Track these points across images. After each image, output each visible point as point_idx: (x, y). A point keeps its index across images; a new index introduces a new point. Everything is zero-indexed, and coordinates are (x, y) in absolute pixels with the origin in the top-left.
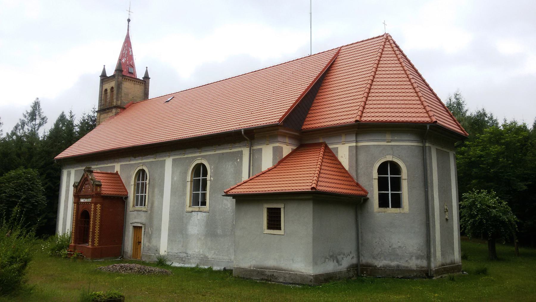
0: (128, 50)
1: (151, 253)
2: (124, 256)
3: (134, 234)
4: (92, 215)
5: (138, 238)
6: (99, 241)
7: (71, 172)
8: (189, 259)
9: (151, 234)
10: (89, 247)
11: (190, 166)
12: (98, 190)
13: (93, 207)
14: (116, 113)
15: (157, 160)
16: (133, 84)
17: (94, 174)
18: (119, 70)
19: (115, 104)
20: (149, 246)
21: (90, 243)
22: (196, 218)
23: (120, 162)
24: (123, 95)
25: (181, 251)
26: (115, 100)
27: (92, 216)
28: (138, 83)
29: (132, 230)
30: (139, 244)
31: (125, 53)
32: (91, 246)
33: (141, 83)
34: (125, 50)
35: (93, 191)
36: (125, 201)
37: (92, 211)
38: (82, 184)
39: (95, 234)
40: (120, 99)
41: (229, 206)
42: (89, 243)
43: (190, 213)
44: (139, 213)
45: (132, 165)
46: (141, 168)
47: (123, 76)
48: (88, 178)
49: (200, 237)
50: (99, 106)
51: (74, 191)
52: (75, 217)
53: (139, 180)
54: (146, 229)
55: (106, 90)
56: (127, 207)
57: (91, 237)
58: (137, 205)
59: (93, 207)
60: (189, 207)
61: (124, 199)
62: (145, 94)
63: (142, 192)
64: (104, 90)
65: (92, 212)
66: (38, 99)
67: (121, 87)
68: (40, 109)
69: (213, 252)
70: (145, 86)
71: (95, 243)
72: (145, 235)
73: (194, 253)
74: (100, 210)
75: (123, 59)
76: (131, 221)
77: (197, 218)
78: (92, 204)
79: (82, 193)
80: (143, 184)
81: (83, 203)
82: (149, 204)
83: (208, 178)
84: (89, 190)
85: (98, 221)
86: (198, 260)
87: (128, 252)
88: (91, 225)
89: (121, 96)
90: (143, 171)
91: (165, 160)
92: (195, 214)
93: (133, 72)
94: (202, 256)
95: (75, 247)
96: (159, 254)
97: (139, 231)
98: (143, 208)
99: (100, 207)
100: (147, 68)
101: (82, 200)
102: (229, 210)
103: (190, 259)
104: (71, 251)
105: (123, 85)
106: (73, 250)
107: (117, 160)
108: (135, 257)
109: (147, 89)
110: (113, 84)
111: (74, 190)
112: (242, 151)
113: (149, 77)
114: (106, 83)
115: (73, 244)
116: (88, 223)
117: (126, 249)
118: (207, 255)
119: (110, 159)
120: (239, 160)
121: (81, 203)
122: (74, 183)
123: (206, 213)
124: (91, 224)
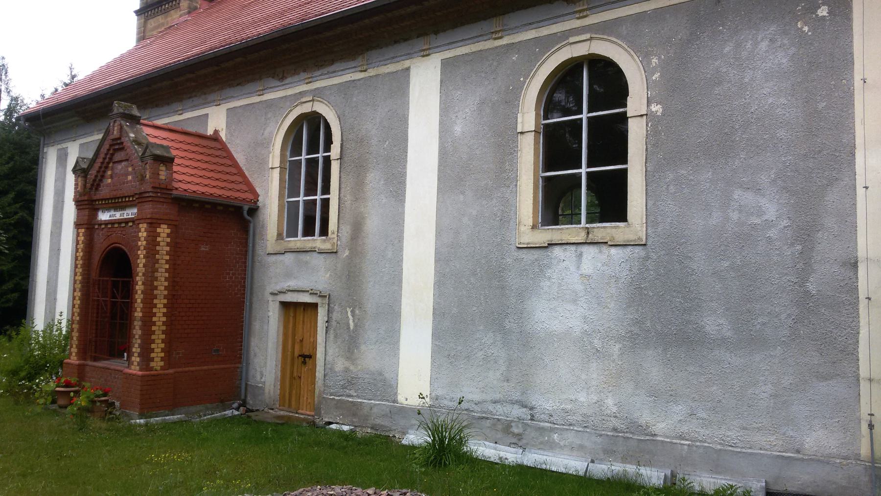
1: (359, 397)
2: (250, 400)
3: (286, 327)
4: (142, 261)
5: (301, 341)
6: (168, 351)
7: (69, 151)
8: (542, 429)
9: (355, 330)
10: (134, 372)
11: (528, 74)
12: (163, 174)
13: (145, 234)
14: (189, 7)
15: (372, 72)
17: (147, 131)
20: (347, 370)
21: (136, 359)
22: (573, 268)
25: (498, 396)
27: (141, 265)
29: (277, 315)
30: (304, 363)
32: (141, 370)
35: (143, 178)
36: (250, 222)
37: (142, 248)
38: (102, 163)
39: (154, 328)
41: (771, 211)
42: (133, 359)
43: (536, 254)
44: (306, 257)
45: (270, 104)
46: (306, 108)
49: (597, 343)
51: (76, 188)
52: (79, 270)
53: (296, 150)
54: (334, 313)
56: (257, 240)
57: (137, 337)
58: (292, 233)
59: (143, 234)
61: (245, 213)
63: (311, 189)
65: (141, 253)
66: (3, 58)
68: (8, 79)
69: (679, 410)
71: (152, 360)
72: (331, 332)
73: (569, 407)
74: (168, 244)
77: (578, 268)
78: (141, 226)
79: (104, 192)
80: (312, 164)
81: (106, 223)
82: (342, 227)
84: (130, 178)
86: (599, 440)
87: (262, 389)
88: (139, 297)
90: (314, 121)
91: (410, 67)
92: (568, 254)
94: (615, 423)
95: (81, 371)
96: (395, 401)
97: (303, 322)
98: (317, 242)
99: (168, 235)
101: (104, 216)
102: (772, 233)
103: (552, 430)
104: (68, 384)
106: (73, 380)
107: (211, 97)
108: (290, 406)
111: (76, 185)
115: (74, 360)
116: (128, 290)
117: (254, 377)
118: (645, 417)
119: (190, 98)
120: (823, 12)
121: (101, 223)
122: (77, 162)
123: (630, 247)
124: (139, 292)
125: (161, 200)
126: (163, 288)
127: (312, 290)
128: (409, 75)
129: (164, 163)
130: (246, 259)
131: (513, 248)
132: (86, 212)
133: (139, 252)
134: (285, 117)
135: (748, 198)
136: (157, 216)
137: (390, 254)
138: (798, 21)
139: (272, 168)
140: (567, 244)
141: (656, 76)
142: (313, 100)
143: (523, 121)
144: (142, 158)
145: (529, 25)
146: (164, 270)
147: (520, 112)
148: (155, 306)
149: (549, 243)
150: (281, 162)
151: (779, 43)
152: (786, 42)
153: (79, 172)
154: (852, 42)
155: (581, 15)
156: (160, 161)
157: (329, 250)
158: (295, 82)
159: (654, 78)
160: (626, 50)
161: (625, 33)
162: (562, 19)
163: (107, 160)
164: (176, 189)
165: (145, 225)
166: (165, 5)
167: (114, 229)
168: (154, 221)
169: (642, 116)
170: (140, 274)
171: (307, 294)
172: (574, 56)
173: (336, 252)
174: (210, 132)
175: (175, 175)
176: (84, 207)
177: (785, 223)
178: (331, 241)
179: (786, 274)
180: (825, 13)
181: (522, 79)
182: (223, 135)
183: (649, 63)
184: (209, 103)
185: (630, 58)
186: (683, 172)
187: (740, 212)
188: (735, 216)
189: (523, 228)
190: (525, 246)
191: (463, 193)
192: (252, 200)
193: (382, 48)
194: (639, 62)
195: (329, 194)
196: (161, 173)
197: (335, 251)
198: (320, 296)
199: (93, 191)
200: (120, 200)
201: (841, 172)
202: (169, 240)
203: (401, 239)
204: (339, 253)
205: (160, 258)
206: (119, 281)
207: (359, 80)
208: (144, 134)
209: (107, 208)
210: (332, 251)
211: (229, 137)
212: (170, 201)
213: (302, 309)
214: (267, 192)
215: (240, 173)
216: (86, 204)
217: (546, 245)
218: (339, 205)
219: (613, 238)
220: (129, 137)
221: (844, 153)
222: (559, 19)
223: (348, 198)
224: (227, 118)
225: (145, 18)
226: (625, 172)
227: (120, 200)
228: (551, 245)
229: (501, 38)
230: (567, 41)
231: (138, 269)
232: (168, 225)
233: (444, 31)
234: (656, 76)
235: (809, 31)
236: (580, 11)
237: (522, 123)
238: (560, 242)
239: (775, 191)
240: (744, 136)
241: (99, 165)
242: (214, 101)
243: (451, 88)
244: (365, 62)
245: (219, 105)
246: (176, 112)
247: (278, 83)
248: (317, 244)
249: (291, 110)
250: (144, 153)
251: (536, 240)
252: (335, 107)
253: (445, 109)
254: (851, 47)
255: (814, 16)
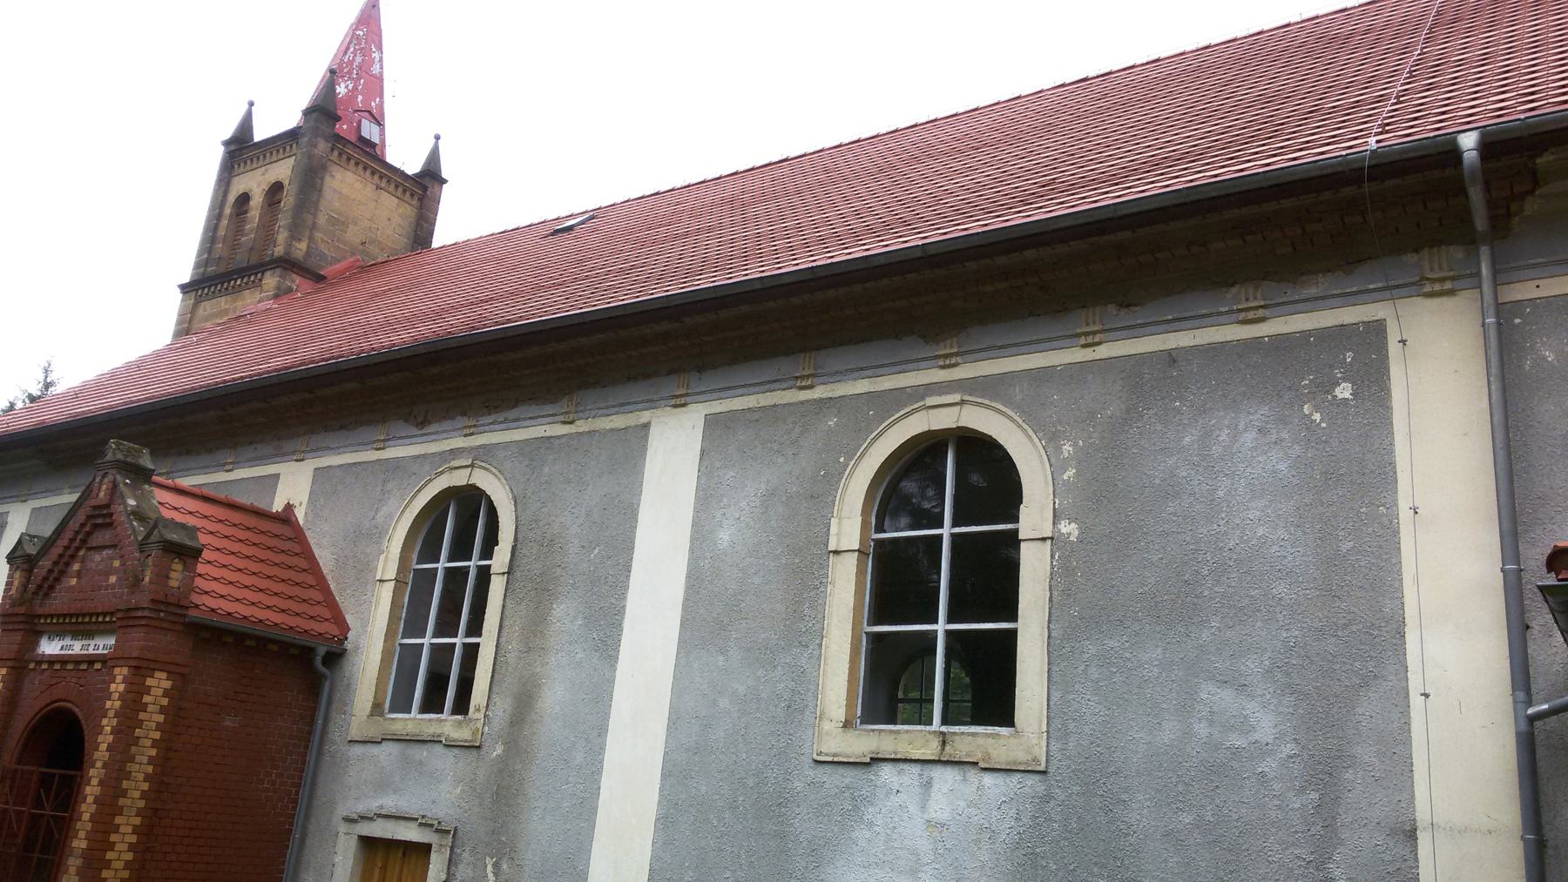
0: (366, 52)
4: (105, 740)
11: (853, 452)
12: (176, 577)
13: (122, 687)
14: (278, 288)
15: (582, 426)
16: (370, 188)
17: (161, 495)
18: (323, 111)
19: (279, 251)
22: (913, 809)
23: (317, 451)
24: (322, 220)
26: (282, 237)
27: (104, 747)
28: (392, 188)
29: (350, 862)
31: (351, 63)
33: (404, 191)
34: (354, 53)
35: (137, 582)
37: (111, 714)
38: (67, 548)
40: (307, 233)
41: (1265, 726)
43: (849, 776)
44: (421, 753)
45: (395, 466)
46: (459, 479)
47: (338, 138)
48: (117, 508)
50: (197, 266)
51: (6, 591)
54: (461, 867)
55: (244, 199)
59: (118, 687)
60: (845, 726)
61: (318, 660)
62: (415, 242)
63: (447, 625)
64: (232, 198)
65: (108, 724)
67: (322, 184)
70: (421, 208)
74: (163, 710)
75: (343, 85)
76: (343, 810)
77: (923, 808)
78: (117, 671)
79: (59, 601)
80: (455, 578)
81: (52, 660)
82: (495, 698)
83: (1034, 518)
84: (113, 579)
85: (136, 787)
88: (87, 809)
89: (314, 223)
91: (646, 426)
92: (906, 779)
93: (376, 139)
98: (446, 724)
99: (166, 693)
100: (437, 138)
101: (50, 647)
102: (1269, 766)
105: (328, 179)
107: (288, 446)
109: (427, 222)
110: (282, 170)
111: (9, 584)
112: (1377, 329)
113: (444, 175)
114: (248, 168)
116: (68, 795)
120: (1344, 391)
122: (19, 542)
123: (1018, 776)
124: (90, 799)
125: (165, 625)
126: (137, 794)
127: (423, 817)
128: (647, 436)
129: (183, 557)
130: (307, 747)
131: (807, 761)
132: (18, 637)
133: (105, 722)
134: (419, 491)
135: (1224, 698)
136: (151, 656)
137: (579, 758)
138: (1305, 403)
139: (380, 581)
140: (906, 760)
141: (1070, 473)
142: (472, 466)
143: (839, 531)
144: (142, 546)
145: (859, 371)
146: (145, 760)
147: (835, 515)
148: (116, 829)
149: (874, 756)
150: (399, 571)
151: (1274, 437)
152: (1285, 435)
153: (19, 561)
154: (1392, 444)
155: (948, 362)
156: (174, 552)
157: (466, 741)
158: (445, 431)
159: (1065, 477)
160: (1020, 426)
161: (1019, 397)
162: (914, 365)
163: (76, 544)
164: (197, 606)
165: (125, 671)
166: (236, 280)
167: (66, 674)
168: (145, 664)
169: (1044, 539)
170: (99, 764)
171: (414, 825)
172: (932, 429)
173: (478, 747)
174: (278, 506)
175: (199, 582)
176: (16, 627)
177: (1288, 749)
178: (471, 725)
179: (1293, 844)
180: (1347, 395)
181: (842, 460)
182: (300, 514)
183: (1058, 449)
184: (283, 455)
185: (1025, 440)
186: (1112, 643)
187: (1211, 723)
188: (1202, 730)
189: (827, 726)
190: (830, 759)
191: (723, 651)
192: (335, 636)
193: (605, 387)
194: (1041, 448)
195: (480, 635)
196: (173, 575)
197: (478, 744)
198: (437, 831)
199: (40, 597)
200: (87, 620)
201: (1383, 665)
202: (165, 702)
203: (602, 731)
204: (484, 749)
205: (142, 735)
206: (54, 775)
207: (559, 437)
208: (155, 502)
209: (58, 633)
210: (471, 744)
211: (310, 519)
212: (180, 628)
213: (400, 854)
214: (365, 623)
215: (321, 584)
216: (19, 622)
217: (868, 760)
218: (495, 658)
219: (987, 757)
220: (126, 505)
221: (1387, 632)
222: (910, 366)
223: (513, 645)
224: (313, 484)
225: (195, 299)
226: (1014, 633)
227: (87, 620)
228: (876, 760)
229: (811, 387)
230: (922, 403)
231: (97, 755)
232: (169, 672)
233: (714, 367)
234: (1070, 473)
235: (1322, 420)
236: (946, 356)
237: (837, 534)
238: (892, 756)
239: (1271, 690)
240: (1216, 589)
241: (60, 550)
242: (294, 453)
243: (718, 464)
244: (573, 408)
245: (302, 460)
246: (221, 466)
247: (416, 431)
248: (445, 729)
249: (430, 480)
250: (147, 537)
251: (849, 751)
252: (510, 480)
253: (705, 499)
254: (1391, 453)
255: (1329, 397)
